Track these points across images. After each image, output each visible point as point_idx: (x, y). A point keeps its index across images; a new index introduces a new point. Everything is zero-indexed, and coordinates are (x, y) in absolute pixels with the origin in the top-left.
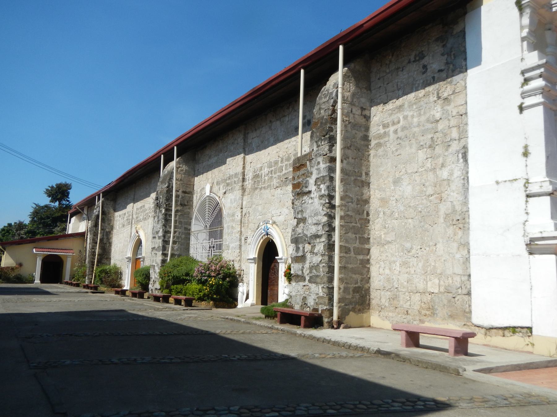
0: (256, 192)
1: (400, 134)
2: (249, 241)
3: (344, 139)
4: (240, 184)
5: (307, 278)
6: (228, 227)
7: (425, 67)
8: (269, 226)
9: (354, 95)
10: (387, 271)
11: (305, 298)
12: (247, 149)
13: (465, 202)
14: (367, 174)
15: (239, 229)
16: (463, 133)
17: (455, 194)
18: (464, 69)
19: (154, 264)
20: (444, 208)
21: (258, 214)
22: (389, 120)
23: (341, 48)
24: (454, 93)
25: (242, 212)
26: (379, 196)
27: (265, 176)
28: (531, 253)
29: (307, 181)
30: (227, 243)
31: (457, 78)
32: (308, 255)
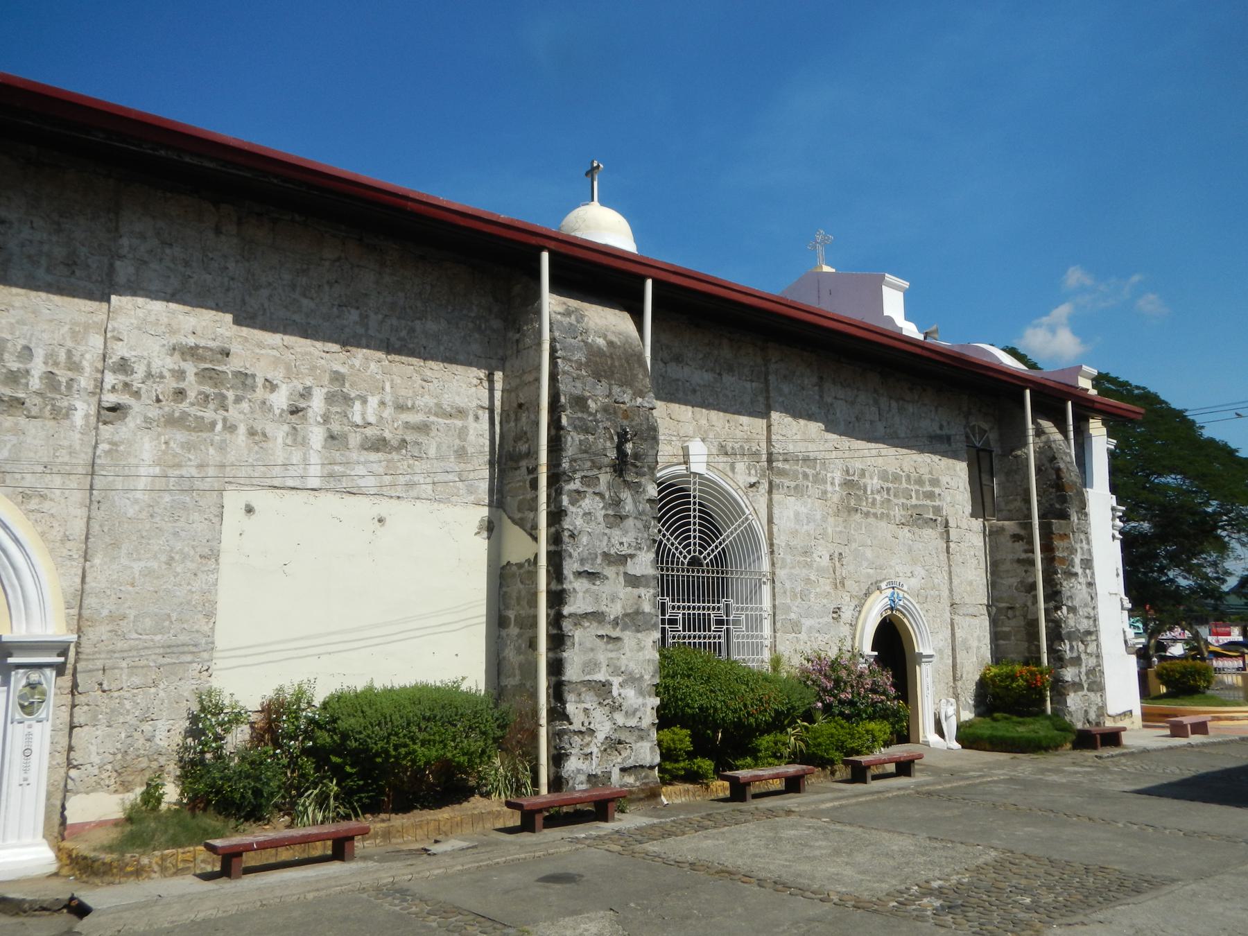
5: (1086, 686)
6: (791, 577)
11: (1086, 712)
19: (600, 676)
21: (865, 564)
27: (872, 493)
29: (1073, 559)
30: (793, 616)
32: (1083, 656)
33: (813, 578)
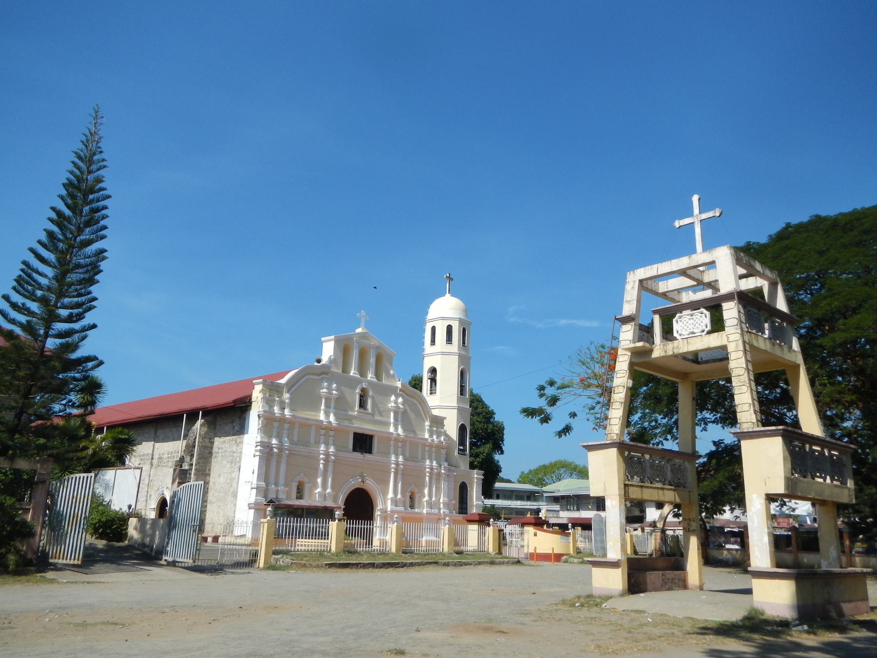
0: (159, 468)
1: (223, 454)
2: (152, 497)
3: (198, 455)
4: (150, 461)
7: (234, 427)
8: (164, 489)
9: (206, 433)
10: (212, 516)
12: (156, 439)
13: (237, 488)
14: (209, 470)
15: (146, 490)
16: (240, 460)
17: (235, 484)
18: (244, 434)
20: (232, 489)
22: (220, 446)
23: (201, 412)
24: (240, 442)
25: (149, 479)
26: (213, 481)
28: (249, 509)
31: (242, 436)
33: (144, 487)
